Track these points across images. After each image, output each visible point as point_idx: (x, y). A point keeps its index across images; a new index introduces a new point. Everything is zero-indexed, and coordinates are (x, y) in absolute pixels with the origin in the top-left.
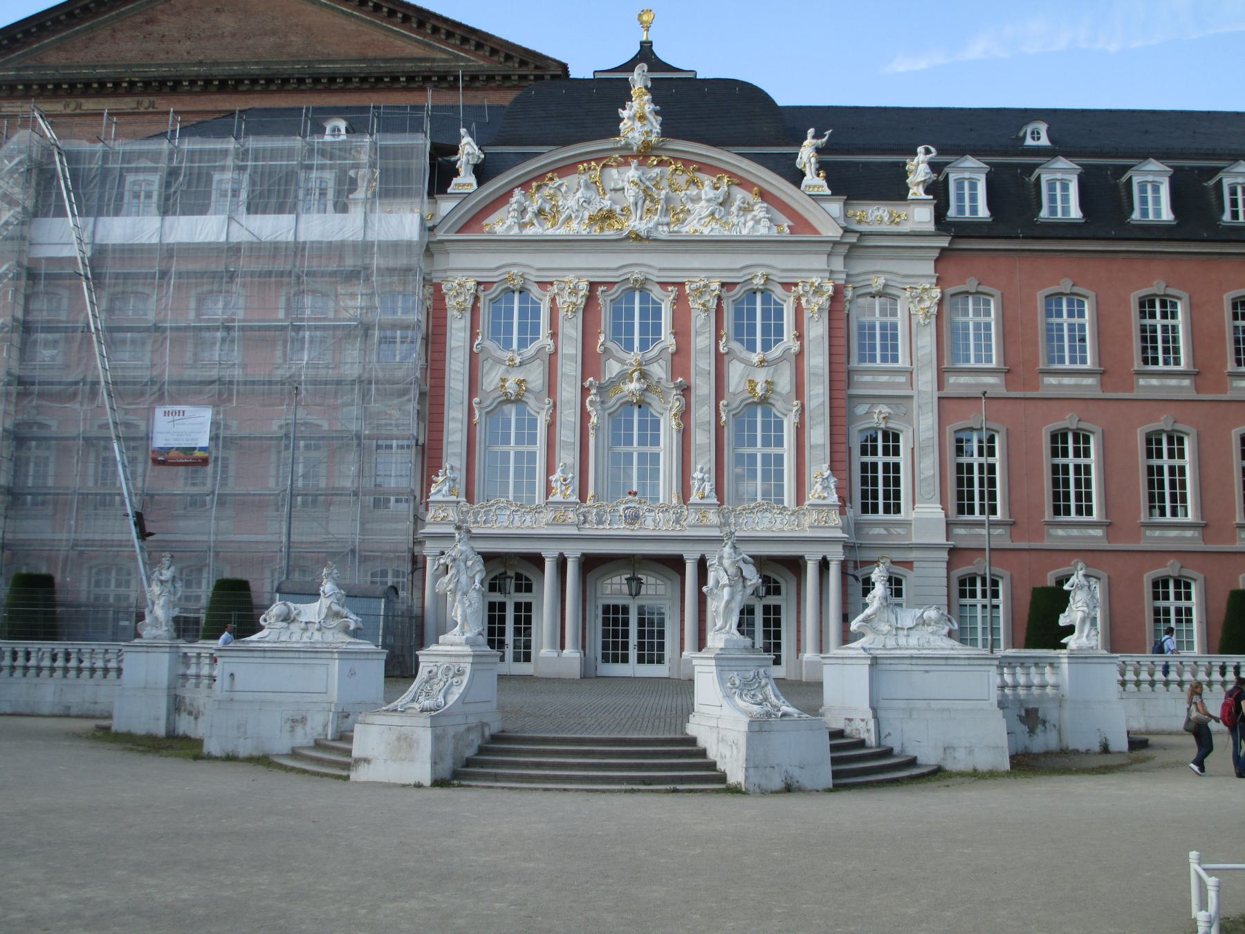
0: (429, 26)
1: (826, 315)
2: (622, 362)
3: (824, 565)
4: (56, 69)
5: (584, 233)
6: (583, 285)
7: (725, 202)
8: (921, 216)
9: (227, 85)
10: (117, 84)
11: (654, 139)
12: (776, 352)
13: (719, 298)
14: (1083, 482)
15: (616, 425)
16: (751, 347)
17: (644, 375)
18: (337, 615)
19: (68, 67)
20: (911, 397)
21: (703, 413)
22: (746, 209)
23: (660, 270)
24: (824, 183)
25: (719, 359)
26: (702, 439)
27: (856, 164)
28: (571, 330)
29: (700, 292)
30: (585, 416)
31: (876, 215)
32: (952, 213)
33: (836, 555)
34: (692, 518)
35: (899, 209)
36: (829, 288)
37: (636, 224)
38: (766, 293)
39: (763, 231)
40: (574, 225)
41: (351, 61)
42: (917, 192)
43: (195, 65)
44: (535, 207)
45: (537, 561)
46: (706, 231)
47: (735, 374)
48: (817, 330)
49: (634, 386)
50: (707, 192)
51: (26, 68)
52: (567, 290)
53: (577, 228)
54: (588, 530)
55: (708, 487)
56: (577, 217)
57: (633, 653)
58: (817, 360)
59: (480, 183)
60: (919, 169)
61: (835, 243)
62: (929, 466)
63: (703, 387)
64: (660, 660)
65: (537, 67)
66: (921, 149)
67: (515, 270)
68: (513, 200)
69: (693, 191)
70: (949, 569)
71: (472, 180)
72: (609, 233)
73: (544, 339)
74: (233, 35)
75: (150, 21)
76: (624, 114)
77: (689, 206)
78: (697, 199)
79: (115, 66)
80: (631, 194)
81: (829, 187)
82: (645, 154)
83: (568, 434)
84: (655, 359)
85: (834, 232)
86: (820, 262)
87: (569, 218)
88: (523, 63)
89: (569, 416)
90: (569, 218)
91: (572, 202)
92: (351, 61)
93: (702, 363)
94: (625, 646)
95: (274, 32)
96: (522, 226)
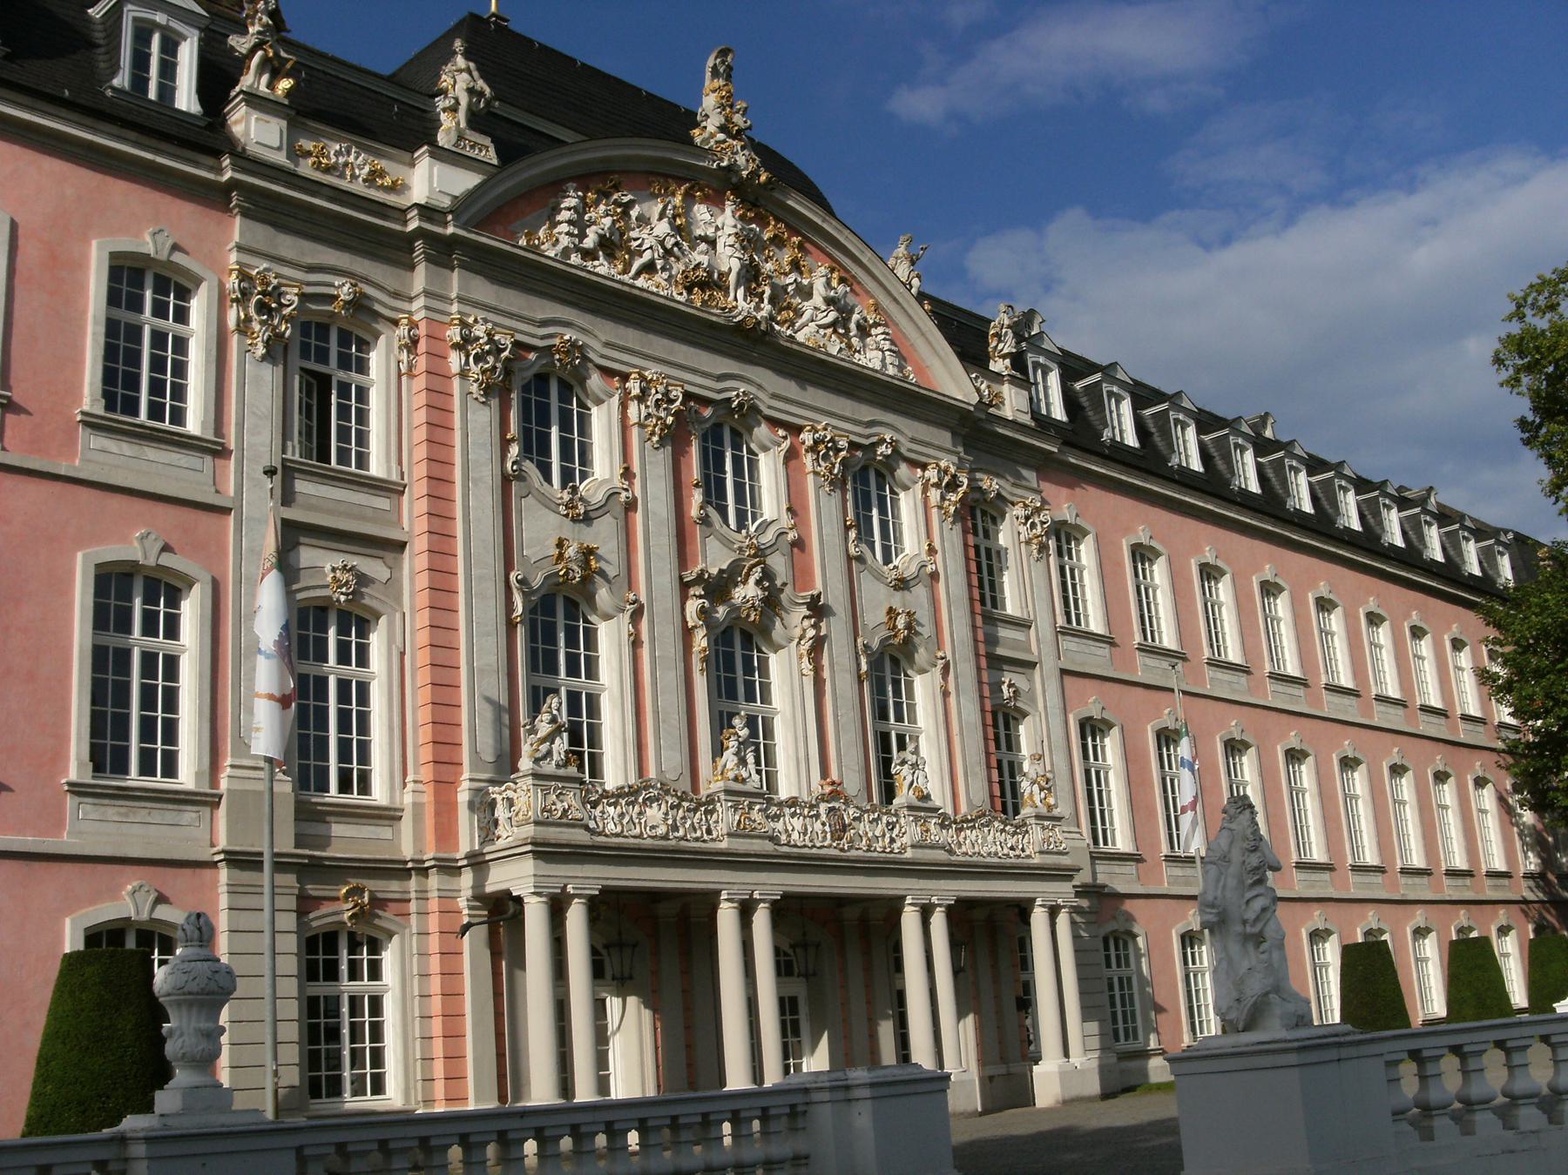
2: (726, 542)
5: (679, 298)
17: (768, 575)
22: (864, 331)
23: (775, 396)
30: (687, 633)
37: (740, 304)
40: (660, 277)
56: (663, 269)
59: (508, 154)
86: (945, 438)
87: (649, 268)
90: (649, 268)
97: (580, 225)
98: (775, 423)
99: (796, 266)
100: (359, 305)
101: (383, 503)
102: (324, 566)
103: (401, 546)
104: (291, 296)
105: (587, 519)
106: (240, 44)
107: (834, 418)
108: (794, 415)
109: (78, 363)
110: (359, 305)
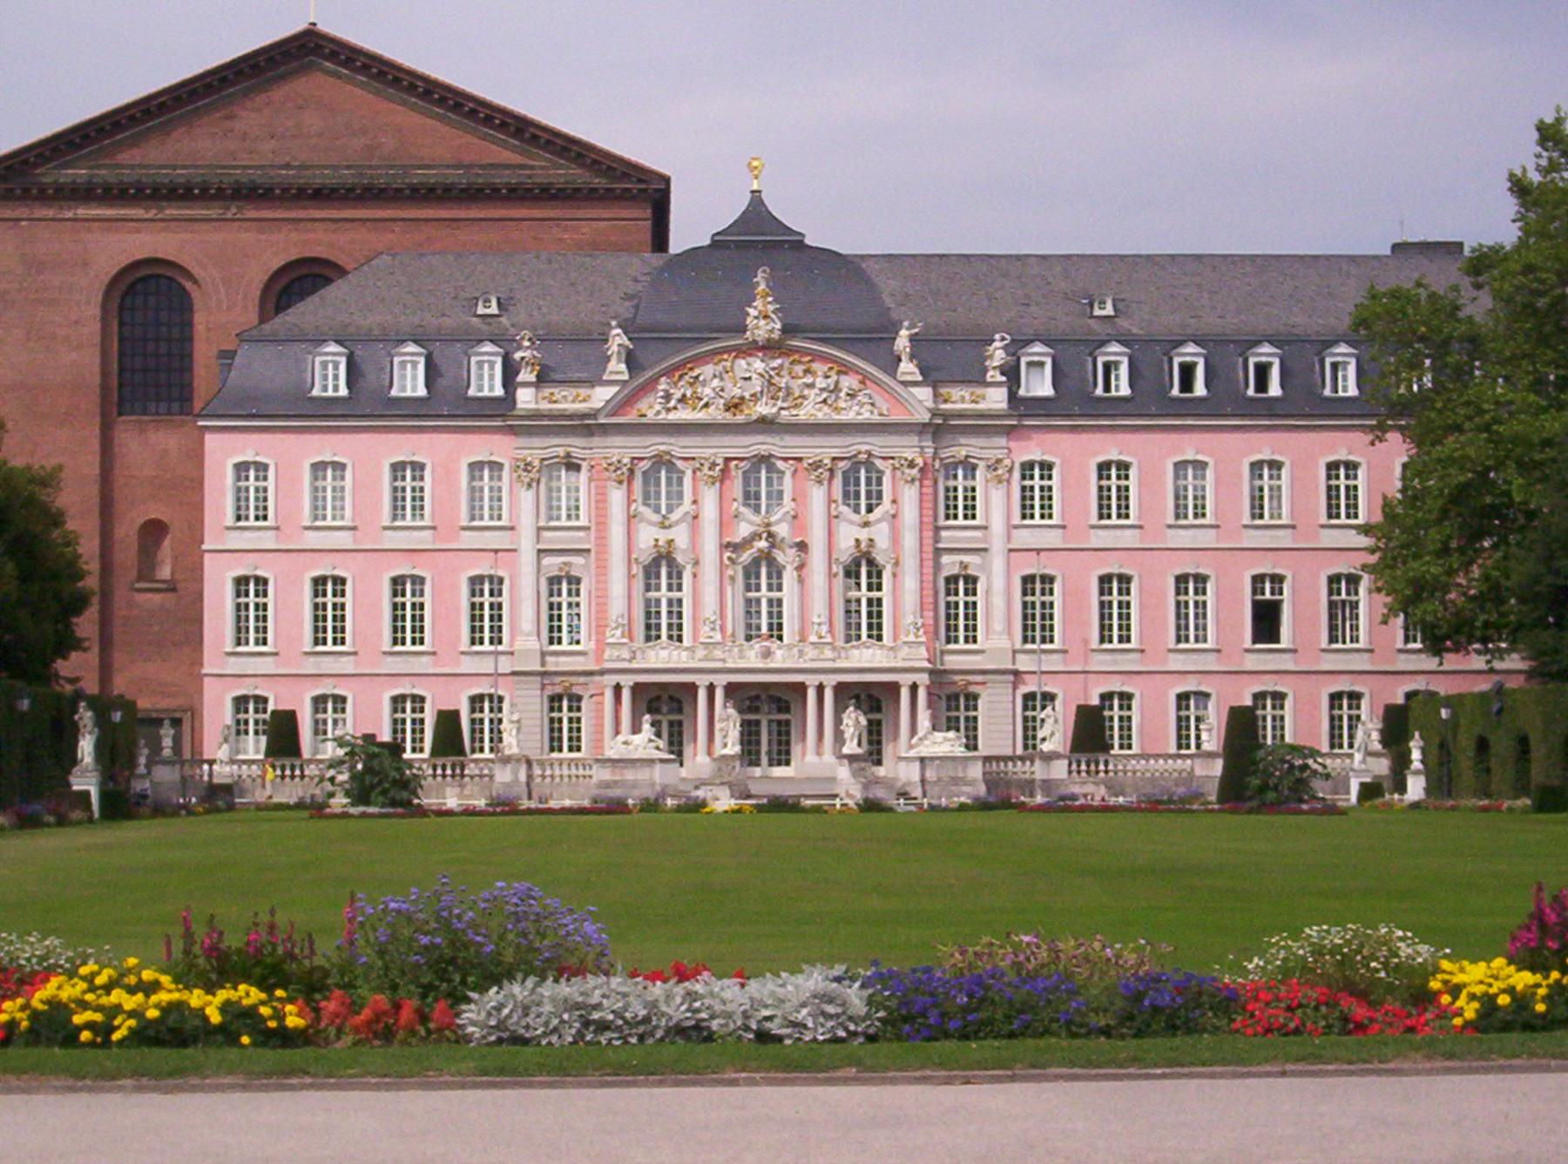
0: (527, 135)
1: (917, 483)
2: (751, 523)
3: (914, 688)
4: (132, 167)
6: (720, 461)
7: (836, 389)
8: (996, 399)
9: (321, 195)
10: (205, 190)
11: (776, 335)
12: (878, 512)
13: (831, 470)
14: (1125, 617)
15: (747, 575)
16: (857, 510)
17: (771, 535)
18: (651, 741)
19: (145, 167)
20: (985, 550)
24: (917, 371)
28: (710, 498)
29: (817, 465)
31: (960, 399)
32: (1022, 392)
33: (923, 679)
34: (811, 653)
35: (979, 391)
36: (920, 461)
37: (763, 409)
38: (869, 465)
39: (866, 415)
40: (711, 409)
41: (448, 167)
42: (994, 375)
43: (281, 167)
44: (678, 395)
45: (692, 688)
46: (820, 415)
48: (910, 495)
49: (763, 544)
50: (821, 382)
51: (99, 167)
52: (707, 465)
53: (716, 414)
54: (730, 665)
55: (825, 628)
57: (764, 759)
60: (997, 354)
61: (924, 425)
64: (788, 763)
65: (640, 181)
66: (997, 336)
67: (662, 448)
68: (661, 387)
69: (808, 380)
70: (1015, 688)
71: (623, 367)
72: (740, 418)
73: (687, 505)
74: (320, 135)
75: (228, 118)
76: (751, 311)
77: (806, 392)
78: (811, 386)
79: (197, 167)
80: (757, 385)
81: (922, 373)
82: (769, 348)
84: (779, 521)
85: (925, 417)
86: (914, 440)
87: (706, 405)
88: (625, 176)
90: (706, 405)
91: (707, 391)
92: (448, 167)
94: (758, 753)
95: (364, 131)
96: (669, 410)
97: (668, 397)
98: (786, 459)
99: (807, 371)
100: (568, 455)
101: (581, 534)
102: (552, 563)
103: (588, 551)
104: (536, 463)
105: (670, 526)
106: (518, 355)
107: (825, 449)
108: (797, 453)
109: (459, 509)
110: (568, 455)
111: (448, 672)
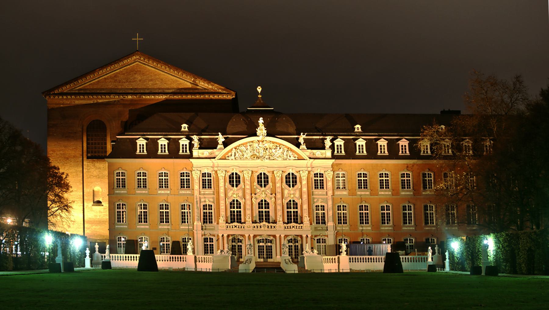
3: (307, 236)
21: (279, 202)
25: (282, 189)
26: (279, 208)
27: (313, 139)
31: (318, 153)
32: (336, 152)
47: (286, 192)
58: (305, 189)
60: (328, 143)
62: (330, 213)
63: (279, 196)
74: (140, 81)
83: (248, 207)
89: (248, 202)
93: (279, 190)
111: (175, 230)
